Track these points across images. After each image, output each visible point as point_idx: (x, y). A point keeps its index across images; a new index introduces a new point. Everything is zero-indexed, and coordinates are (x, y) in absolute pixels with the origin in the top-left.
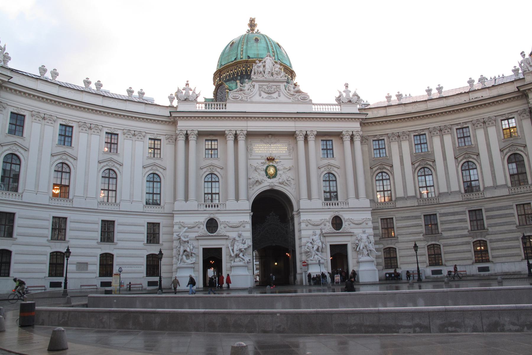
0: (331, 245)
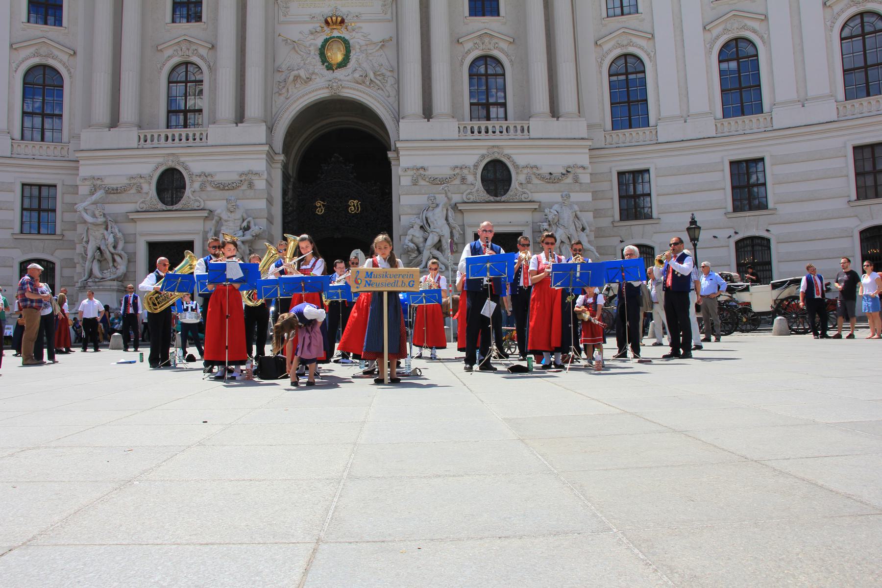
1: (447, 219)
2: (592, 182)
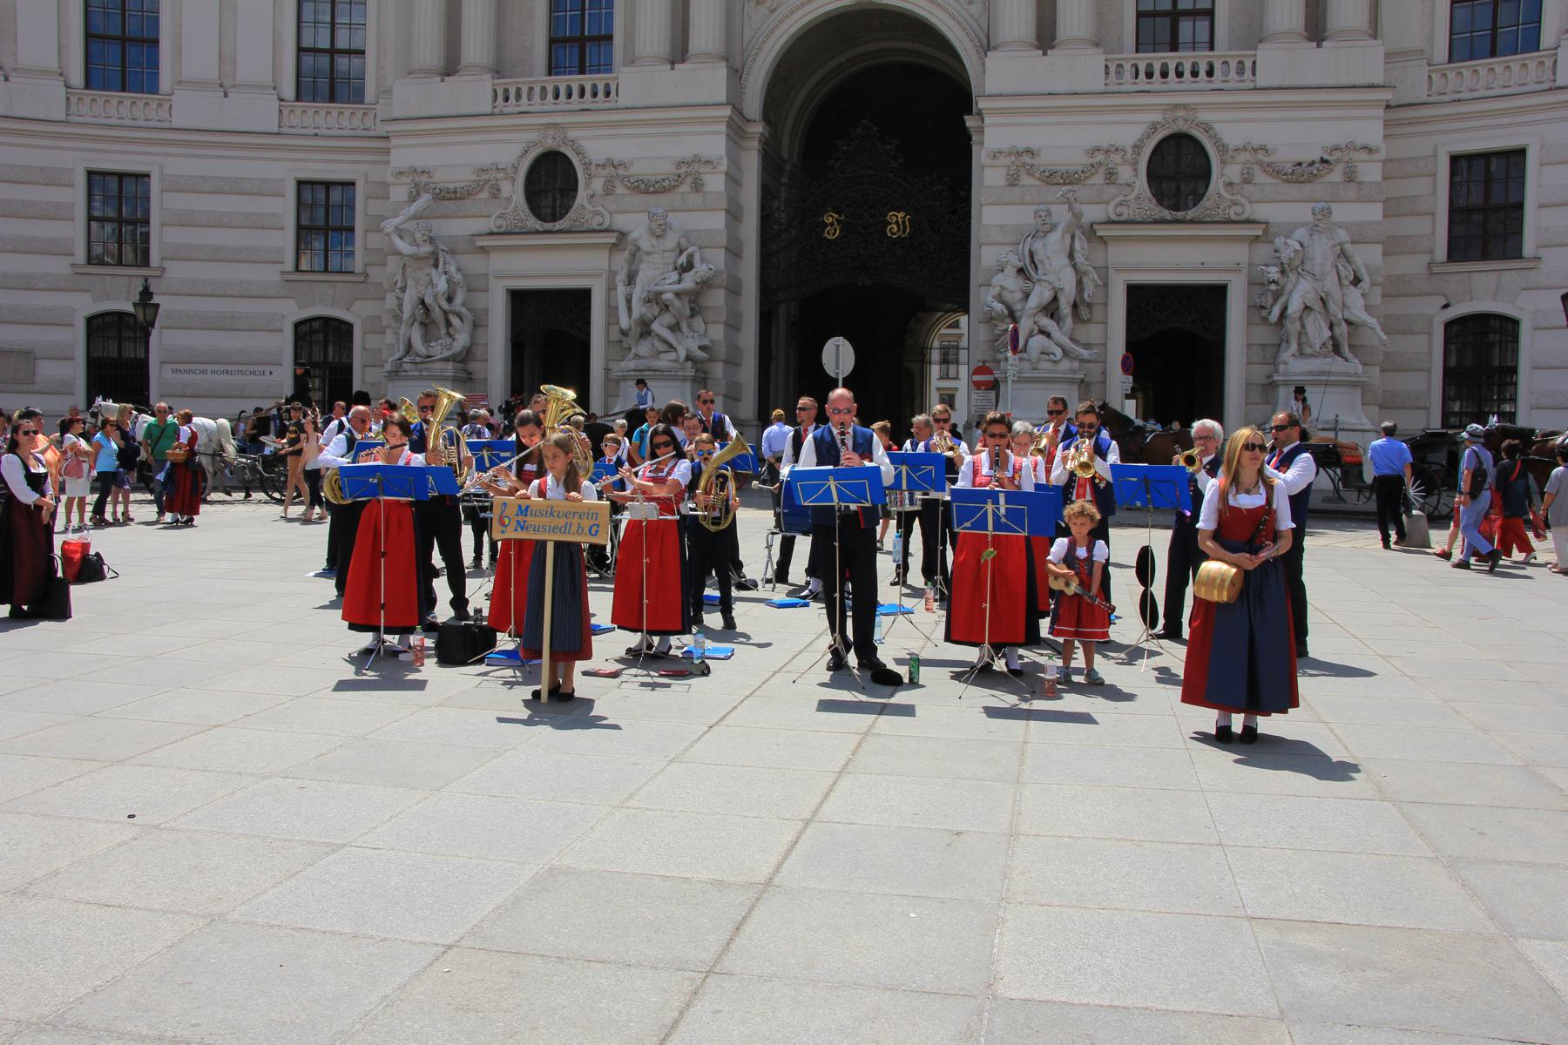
0: (1134, 291)
1: (1071, 256)
2: (1384, 179)
